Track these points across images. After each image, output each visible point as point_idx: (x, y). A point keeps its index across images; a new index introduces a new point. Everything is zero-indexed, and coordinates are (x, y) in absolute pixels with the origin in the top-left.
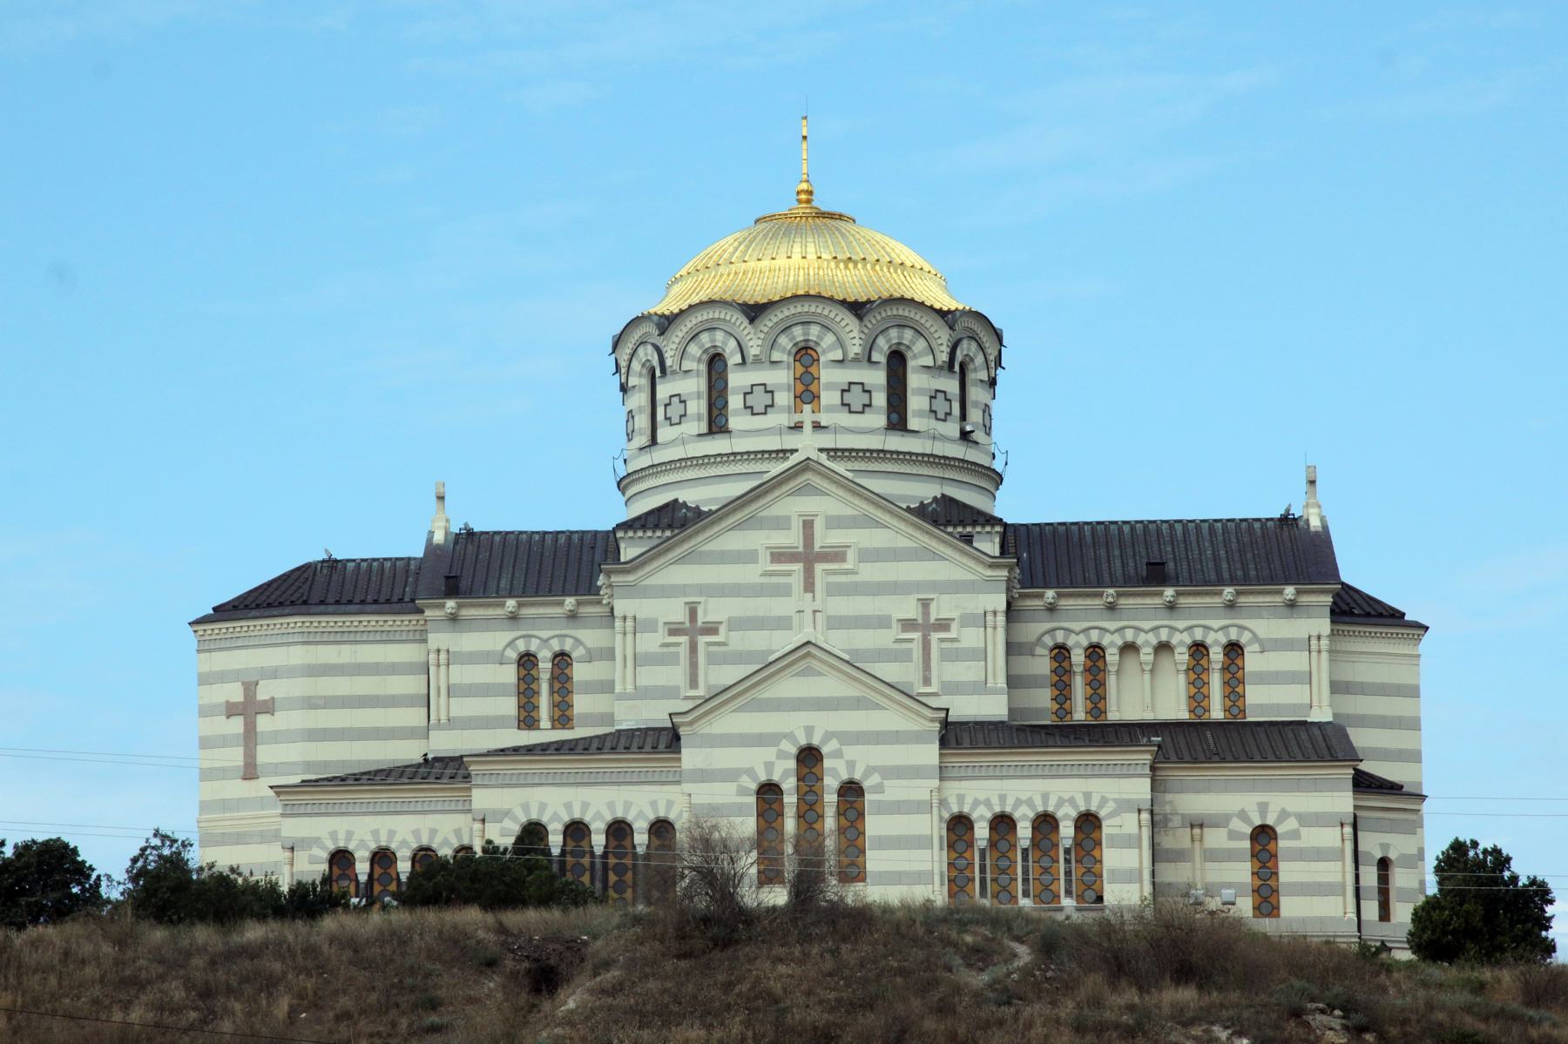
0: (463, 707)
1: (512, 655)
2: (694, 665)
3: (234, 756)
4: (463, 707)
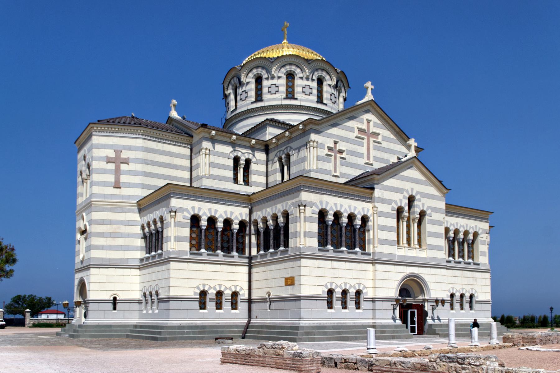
0: (215, 172)
1: (232, 156)
2: (335, 164)
3: (111, 178)
4: (215, 172)
